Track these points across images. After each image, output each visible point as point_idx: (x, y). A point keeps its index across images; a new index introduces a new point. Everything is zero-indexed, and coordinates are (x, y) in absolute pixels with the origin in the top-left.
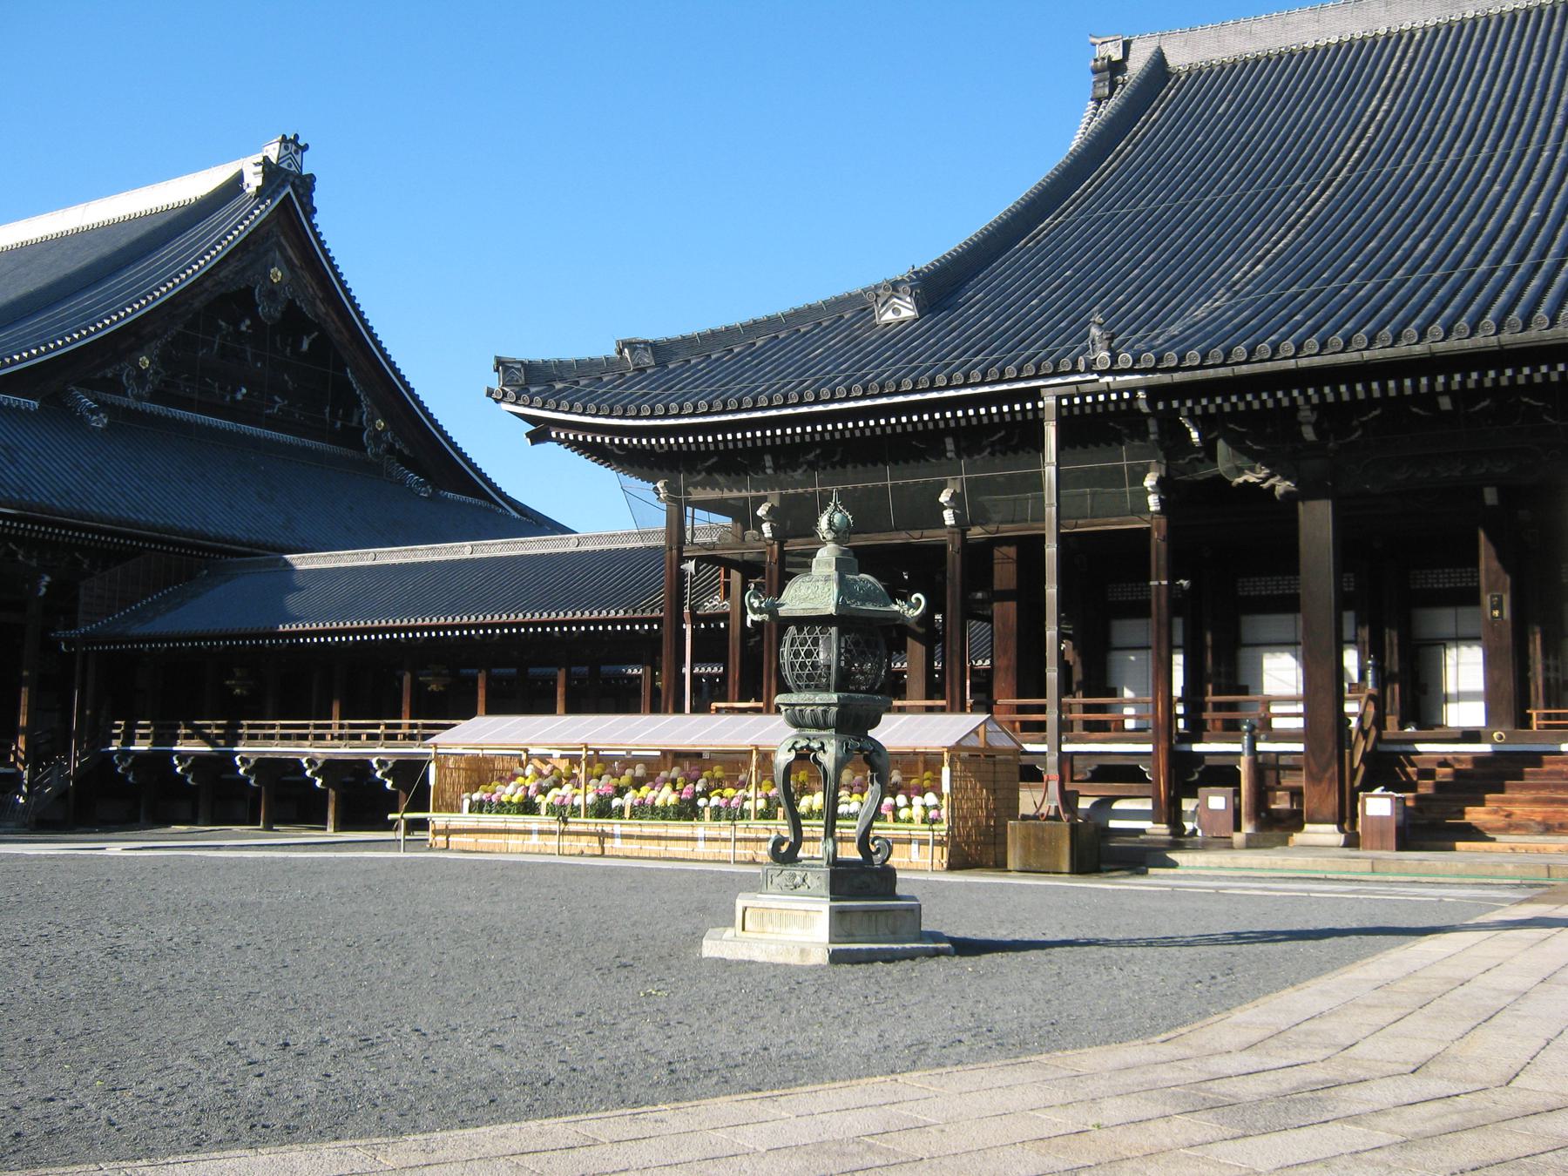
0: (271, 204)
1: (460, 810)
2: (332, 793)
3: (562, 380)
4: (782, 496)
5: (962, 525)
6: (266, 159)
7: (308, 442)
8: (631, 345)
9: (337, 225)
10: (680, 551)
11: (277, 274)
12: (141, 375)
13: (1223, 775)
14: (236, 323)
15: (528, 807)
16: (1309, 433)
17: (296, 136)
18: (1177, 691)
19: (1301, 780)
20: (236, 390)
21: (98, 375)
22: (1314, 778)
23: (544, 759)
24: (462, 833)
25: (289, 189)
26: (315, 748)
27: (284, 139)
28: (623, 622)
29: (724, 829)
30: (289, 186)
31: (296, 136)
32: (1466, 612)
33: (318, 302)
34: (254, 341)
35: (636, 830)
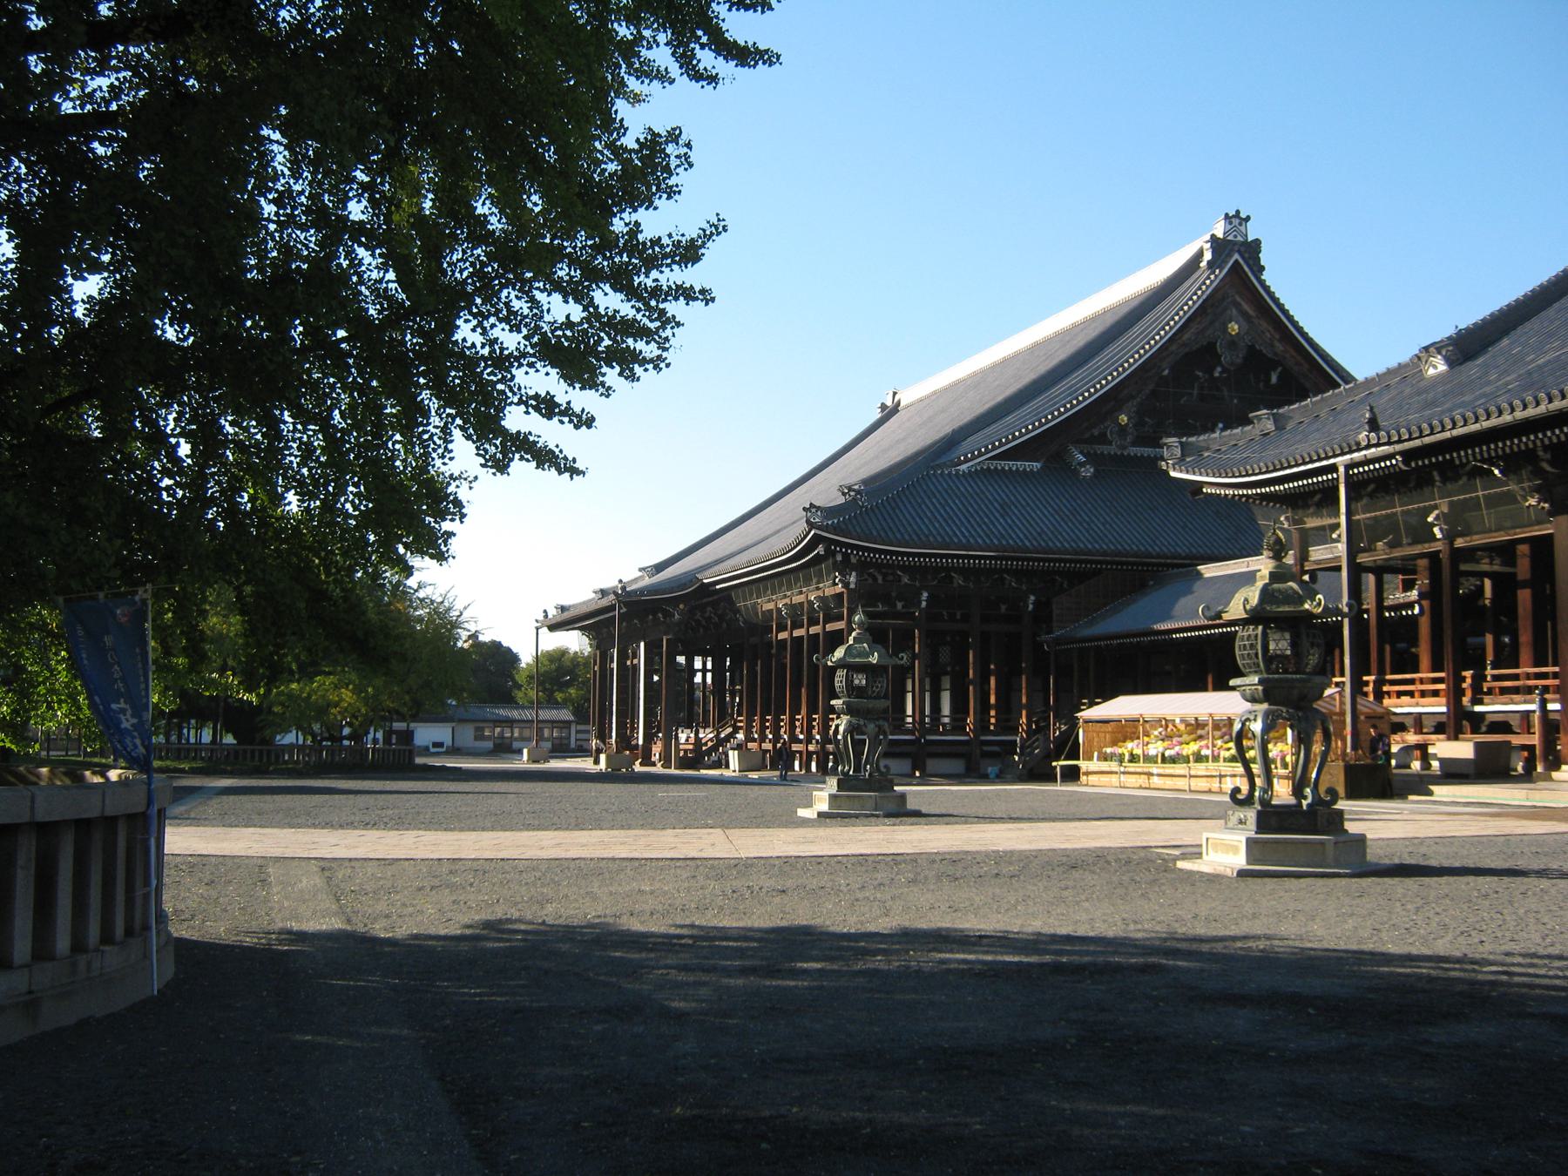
0: (1220, 274)
3: (1208, 449)
4: (1451, 504)
5: (1450, 537)
6: (1213, 236)
9: (1284, 279)
10: (1302, 566)
11: (1234, 328)
12: (1123, 430)
14: (1210, 371)
17: (1238, 212)
18: (909, 696)
21: (1087, 435)
25: (1236, 256)
31: (1238, 212)
33: (1277, 344)
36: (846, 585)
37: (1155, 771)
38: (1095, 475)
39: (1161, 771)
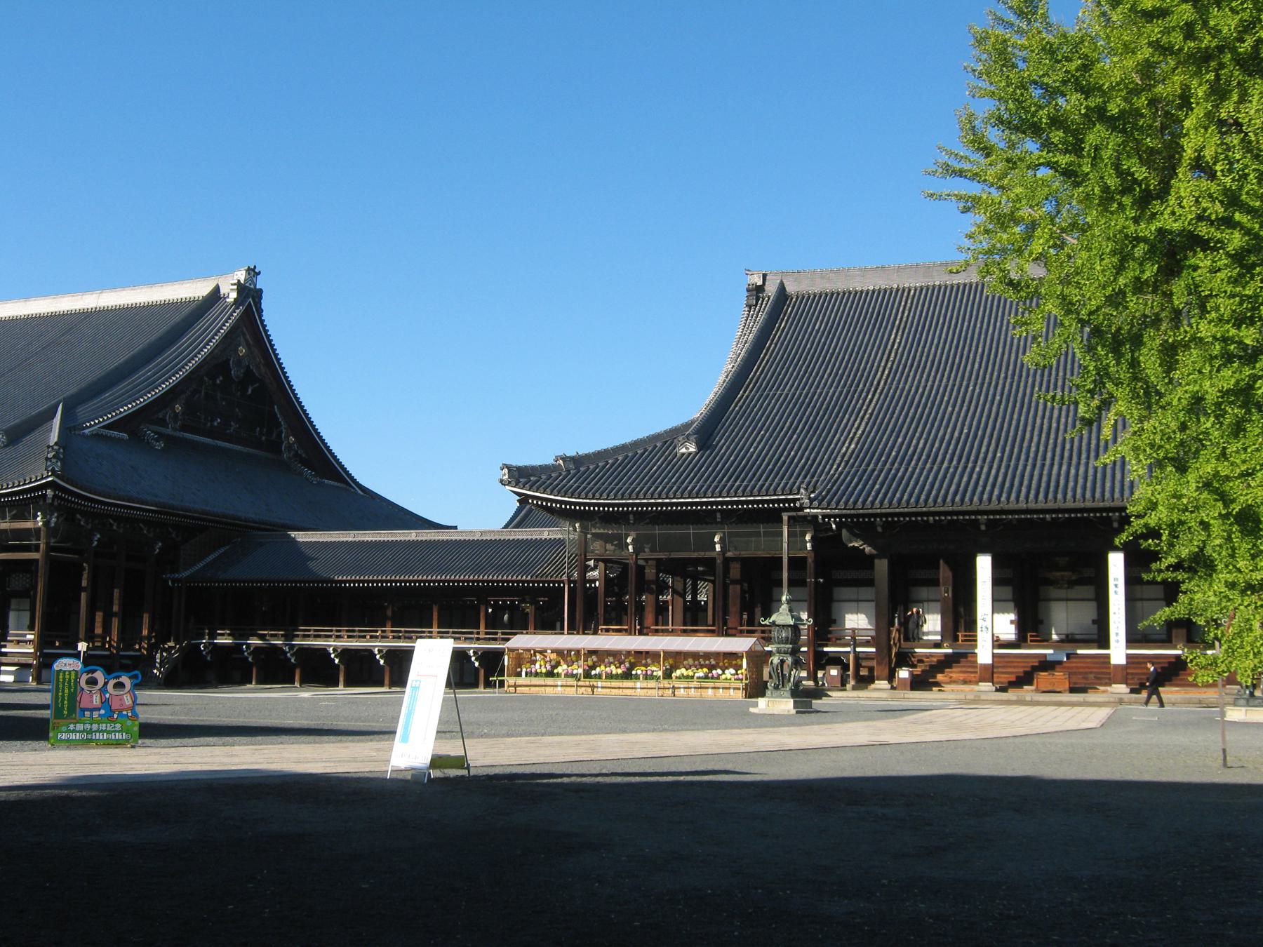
1: (519, 675)
2: (342, 667)
7: (252, 451)
8: (564, 458)
11: (242, 351)
12: (176, 415)
13: (836, 660)
15: (550, 674)
16: (879, 529)
19: (874, 663)
20: (212, 421)
22: (878, 663)
23: (543, 652)
24: (520, 685)
26: (334, 643)
27: (249, 270)
28: (528, 582)
29: (652, 684)
30: (250, 295)
32: (932, 589)
34: (228, 388)
35: (608, 684)
36: (46, 524)
37: (600, 684)
38: (163, 449)
39: (604, 684)
